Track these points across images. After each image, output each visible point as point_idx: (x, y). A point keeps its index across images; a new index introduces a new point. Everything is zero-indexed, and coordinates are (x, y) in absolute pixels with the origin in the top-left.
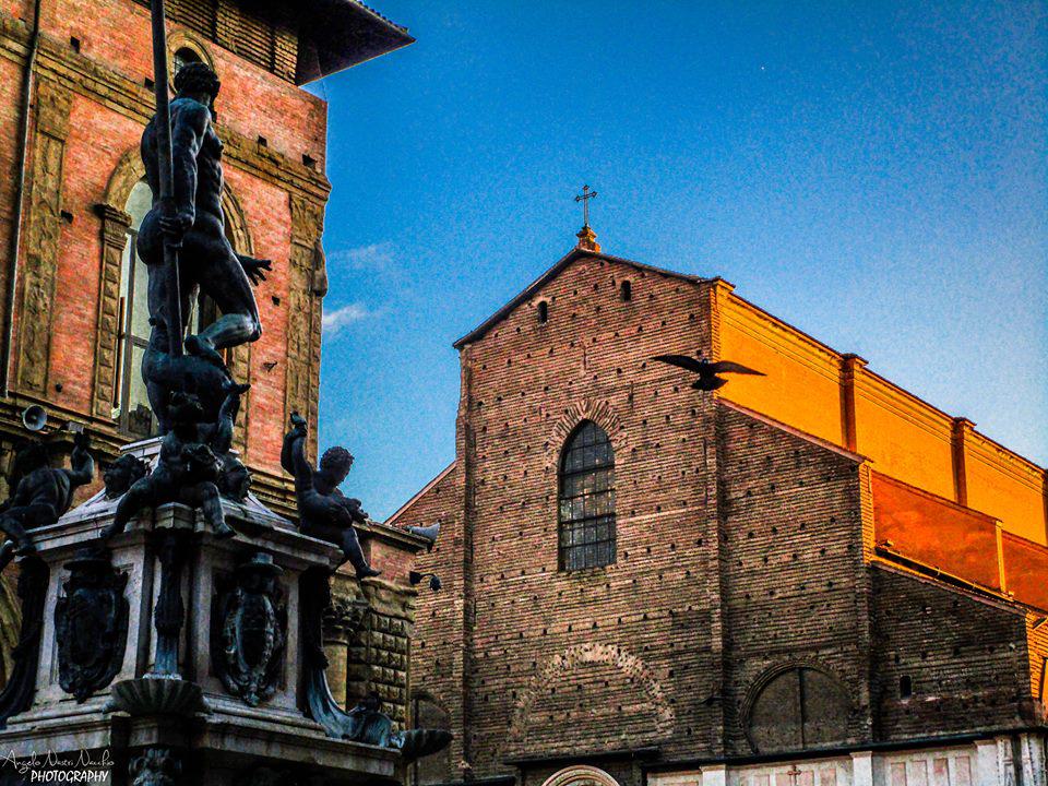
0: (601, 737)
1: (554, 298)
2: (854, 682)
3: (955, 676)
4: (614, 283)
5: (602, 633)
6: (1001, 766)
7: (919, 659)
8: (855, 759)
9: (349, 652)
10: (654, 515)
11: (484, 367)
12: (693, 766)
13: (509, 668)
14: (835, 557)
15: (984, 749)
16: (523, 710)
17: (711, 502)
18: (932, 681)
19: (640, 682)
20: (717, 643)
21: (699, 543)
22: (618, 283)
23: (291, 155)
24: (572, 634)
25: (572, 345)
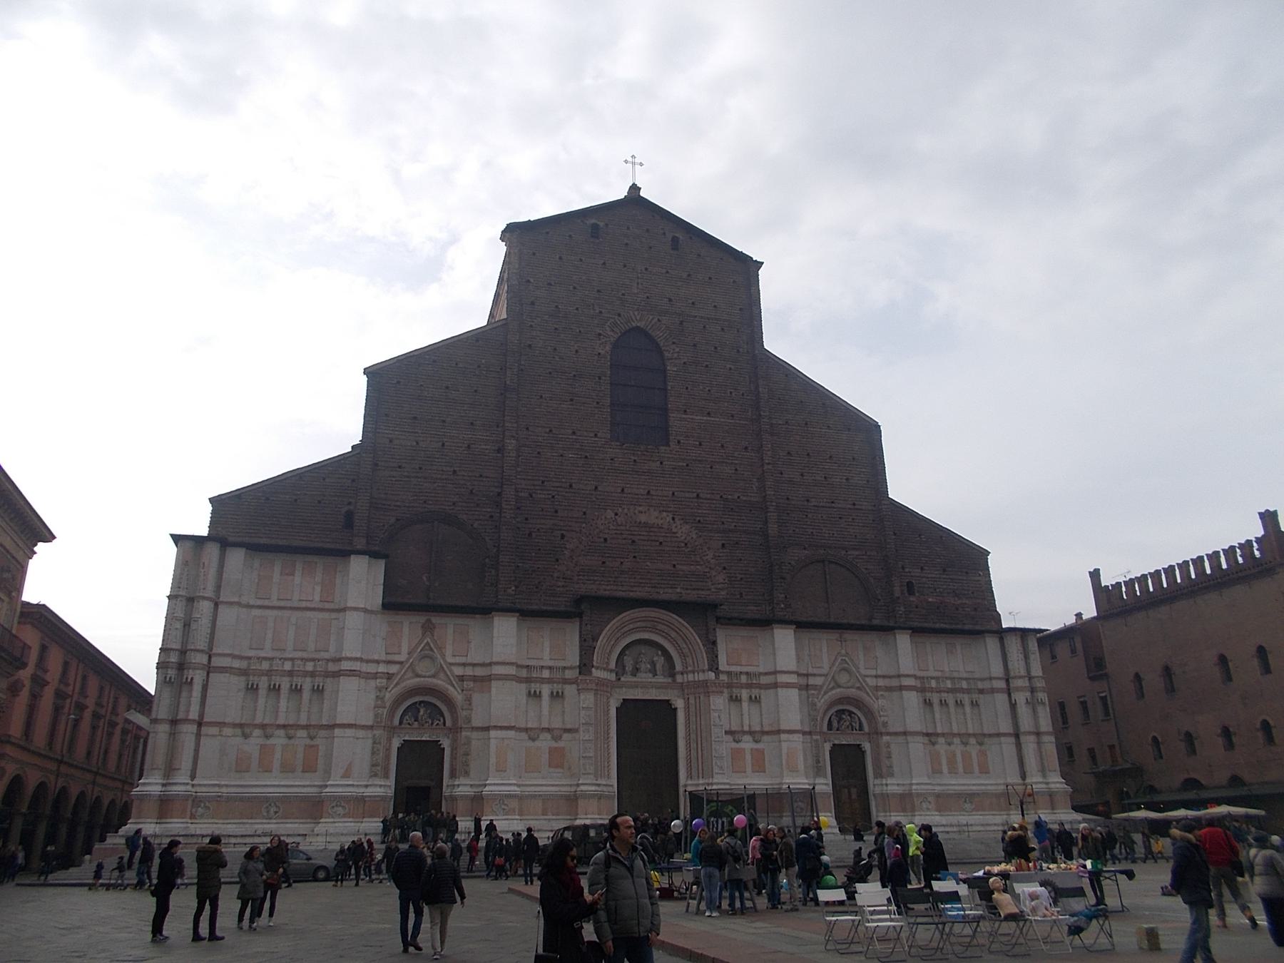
0: (655, 587)
1: (607, 225)
3: (945, 587)
4: (664, 234)
7: (919, 571)
8: (897, 635)
10: (705, 418)
11: (534, 254)
13: (556, 512)
16: (572, 550)
17: (764, 420)
18: (929, 588)
21: (746, 448)
24: (625, 495)
25: (625, 266)
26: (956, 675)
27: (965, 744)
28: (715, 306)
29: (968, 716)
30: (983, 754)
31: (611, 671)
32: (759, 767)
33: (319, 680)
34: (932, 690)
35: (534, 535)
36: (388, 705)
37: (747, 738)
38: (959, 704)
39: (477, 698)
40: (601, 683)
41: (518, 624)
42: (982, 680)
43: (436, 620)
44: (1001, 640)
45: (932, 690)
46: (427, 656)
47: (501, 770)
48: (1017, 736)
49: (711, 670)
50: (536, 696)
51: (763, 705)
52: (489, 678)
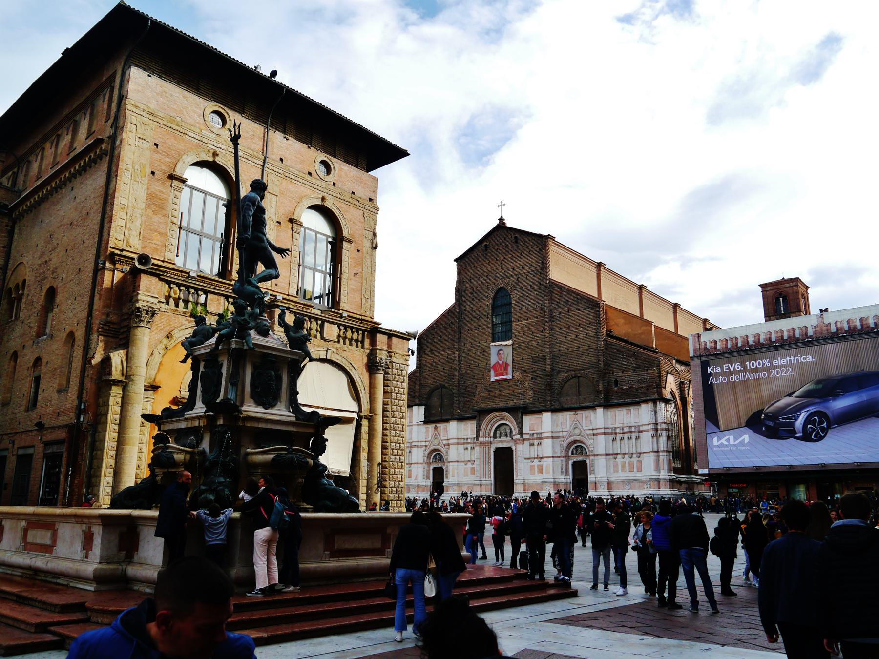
2: (598, 382)
4: (511, 237)
6: (650, 412)
9: (384, 377)
12: (539, 412)
14: (591, 336)
15: (643, 406)
20: (548, 368)
22: (513, 237)
23: (364, 197)
26: (629, 425)
34: (616, 434)
36: (426, 455)
37: (536, 460)
40: (481, 443)
41: (457, 424)
43: (438, 425)
45: (616, 434)
52: (448, 445)
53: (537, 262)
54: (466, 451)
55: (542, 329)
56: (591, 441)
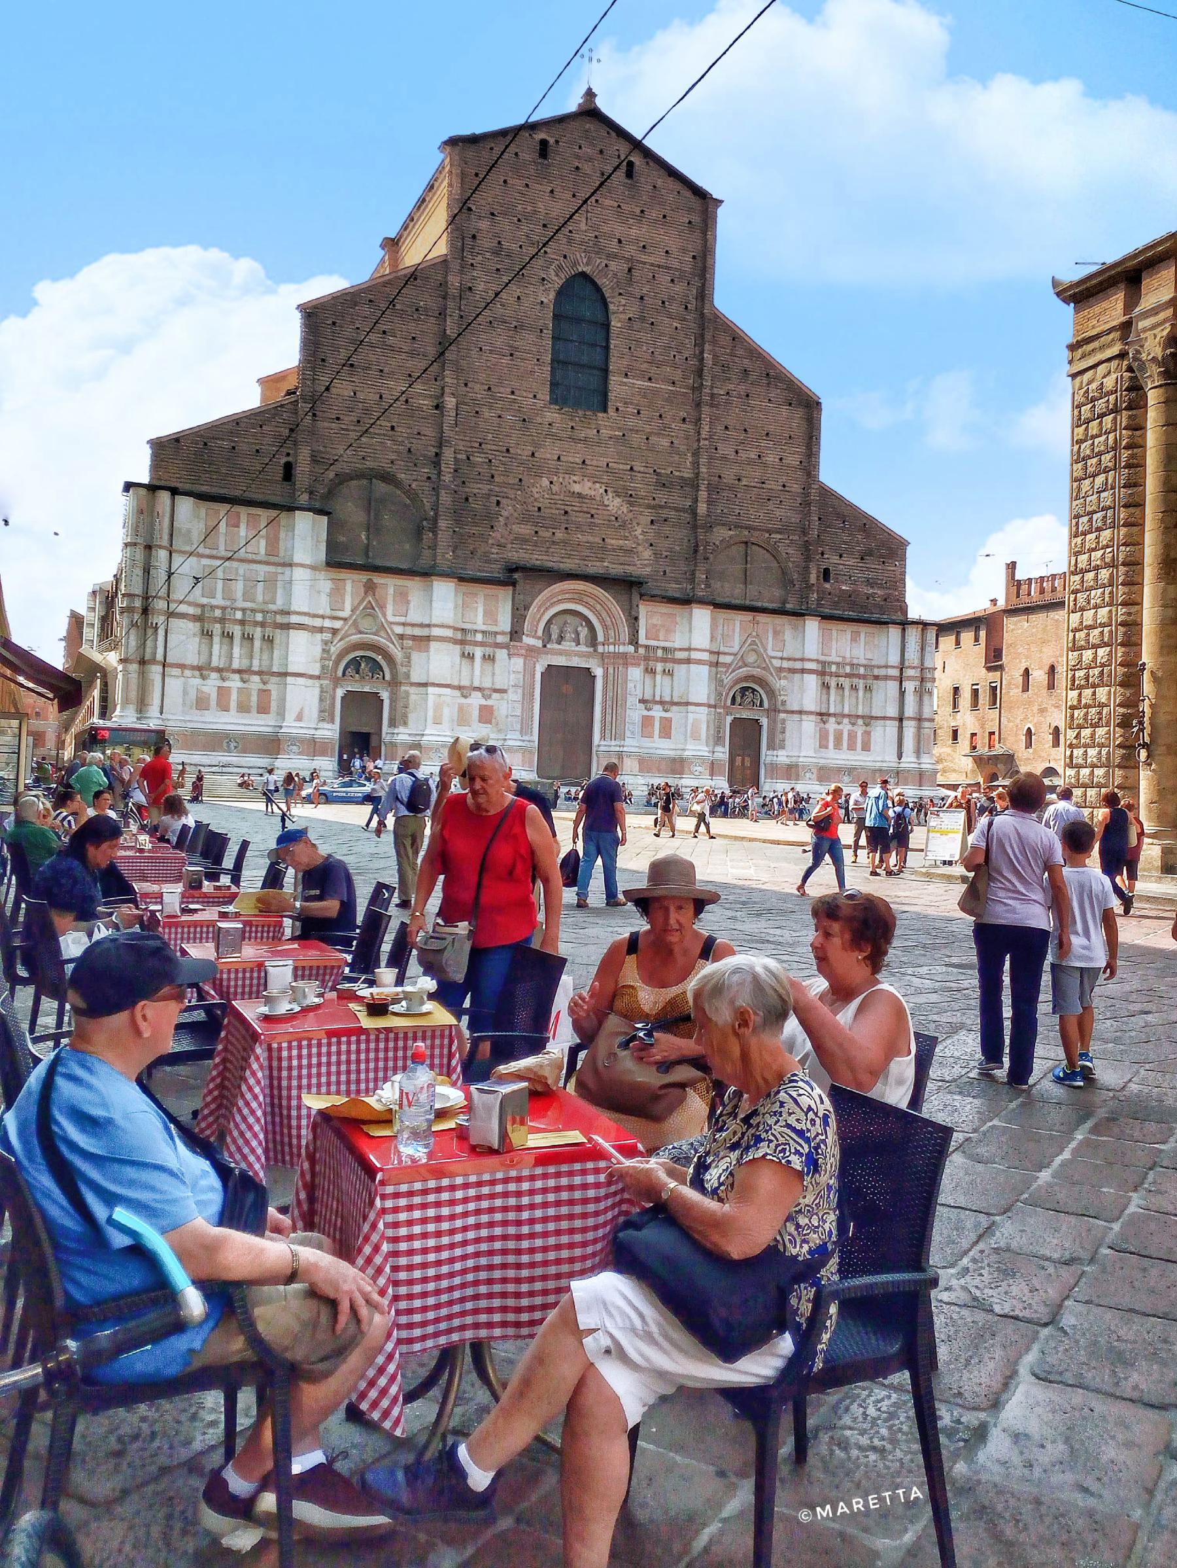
1: (557, 142)
5: (590, 470)
13: (493, 477)
19: (624, 522)
21: (684, 420)
25: (574, 196)
26: (855, 661)
27: (853, 724)
28: (667, 252)
29: (861, 700)
30: (867, 734)
31: (539, 638)
32: (666, 732)
33: (269, 631)
34: (831, 674)
35: (470, 500)
37: (658, 707)
38: (854, 688)
39: (415, 656)
40: (531, 649)
42: (879, 667)
43: (379, 579)
44: (904, 630)
45: (831, 674)
46: (370, 611)
47: (437, 721)
48: (901, 720)
49: (630, 643)
50: (471, 657)
51: (675, 678)
52: (428, 639)
53: (684, 250)
54: (465, 661)
55: (683, 414)
56: (783, 682)
